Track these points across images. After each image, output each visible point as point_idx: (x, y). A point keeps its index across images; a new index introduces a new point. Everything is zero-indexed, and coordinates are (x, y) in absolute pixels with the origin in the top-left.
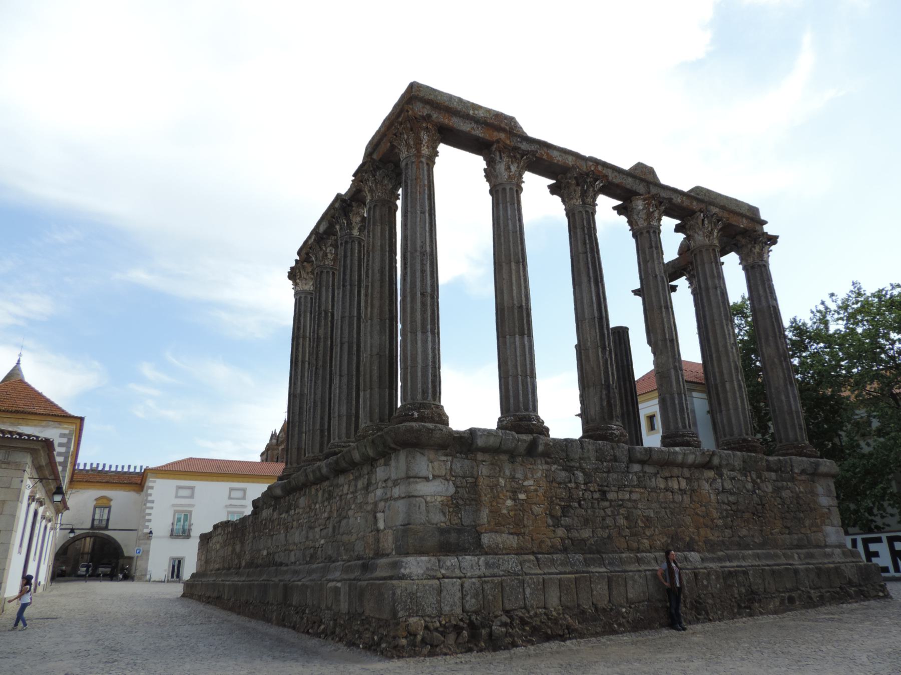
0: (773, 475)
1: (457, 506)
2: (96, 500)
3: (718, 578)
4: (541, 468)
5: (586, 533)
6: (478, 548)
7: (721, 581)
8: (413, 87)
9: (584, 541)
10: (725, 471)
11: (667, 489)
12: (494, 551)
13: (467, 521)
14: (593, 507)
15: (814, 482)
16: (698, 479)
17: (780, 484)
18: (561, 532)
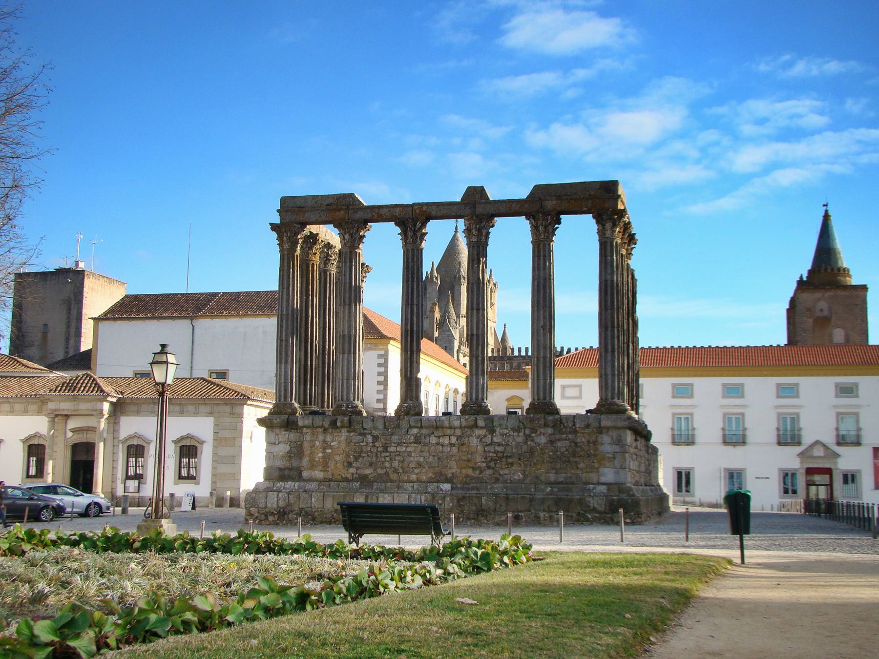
0: (550, 431)
1: (290, 457)
2: (508, 400)
3: (452, 500)
4: (344, 433)
5: (368, 471)
6: (300, 478)
7: (455, 501)
8: (284, 200)
9: (366, 476)
10: (498, 430)
11: (438, 444)
12: (310, 480)
13: (294, 465)
14: (377, 455)
15: (601, 433)
16: (468, 437)
17: (558, 437)
18: (352, 470)
